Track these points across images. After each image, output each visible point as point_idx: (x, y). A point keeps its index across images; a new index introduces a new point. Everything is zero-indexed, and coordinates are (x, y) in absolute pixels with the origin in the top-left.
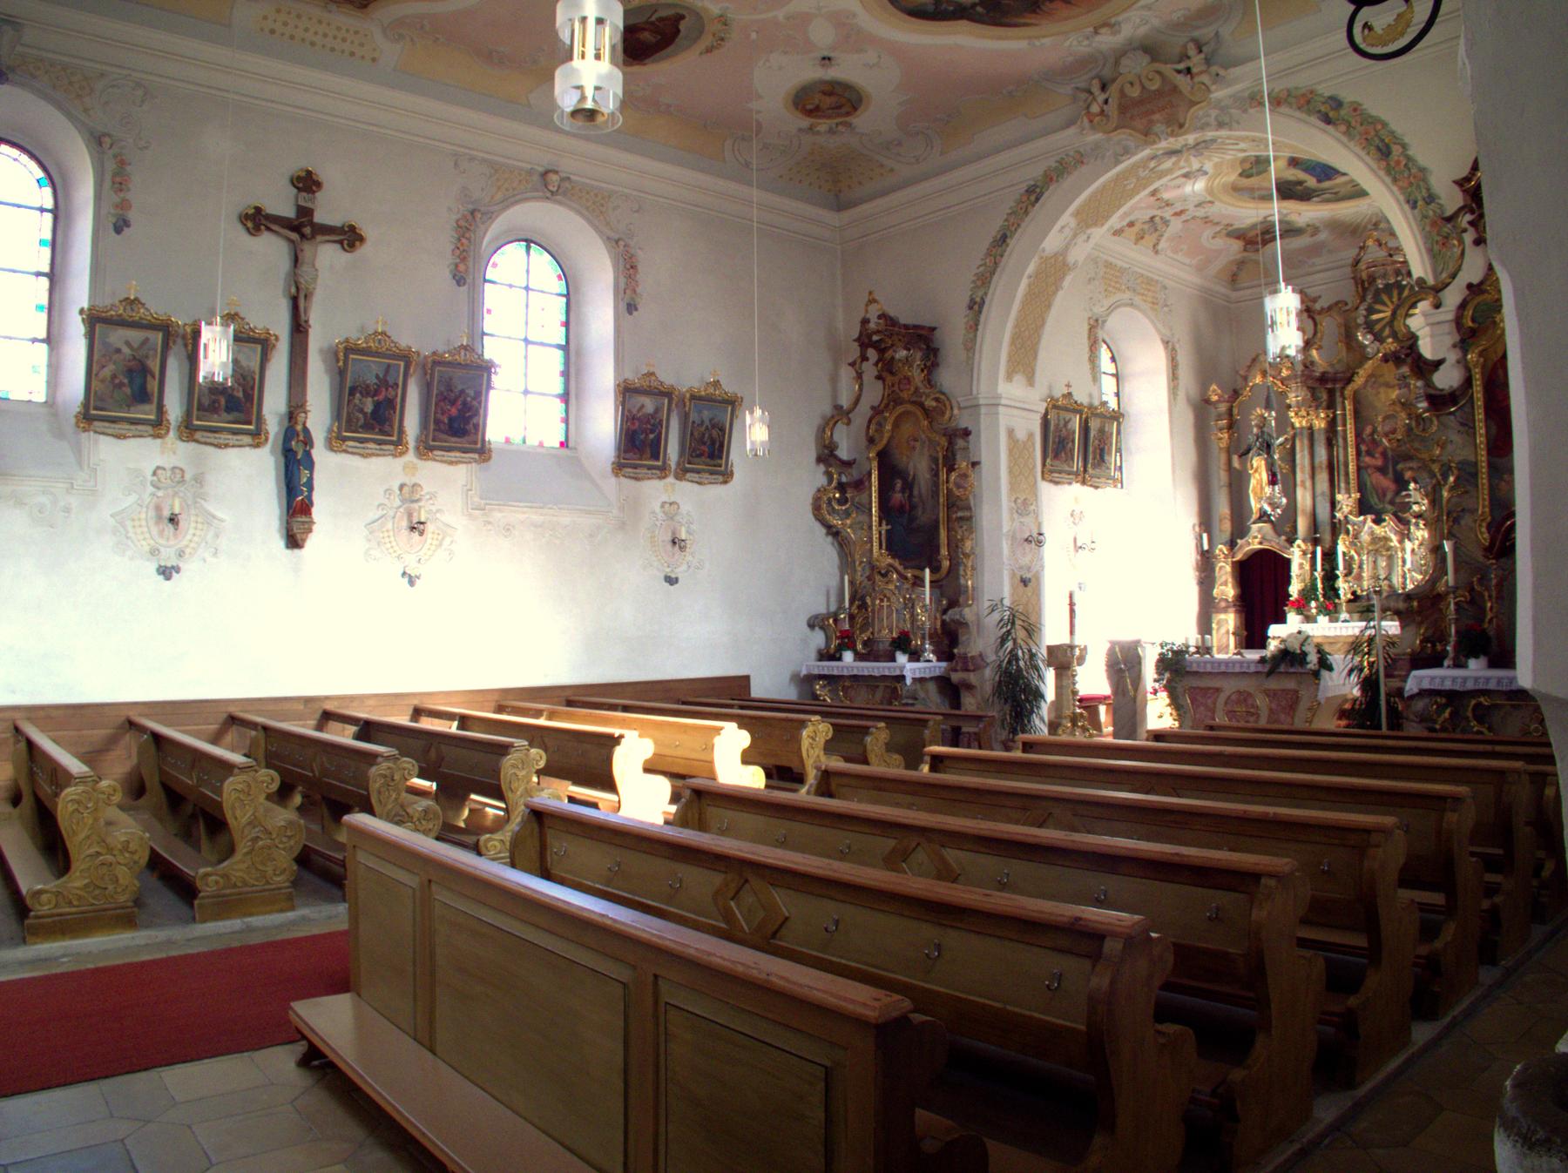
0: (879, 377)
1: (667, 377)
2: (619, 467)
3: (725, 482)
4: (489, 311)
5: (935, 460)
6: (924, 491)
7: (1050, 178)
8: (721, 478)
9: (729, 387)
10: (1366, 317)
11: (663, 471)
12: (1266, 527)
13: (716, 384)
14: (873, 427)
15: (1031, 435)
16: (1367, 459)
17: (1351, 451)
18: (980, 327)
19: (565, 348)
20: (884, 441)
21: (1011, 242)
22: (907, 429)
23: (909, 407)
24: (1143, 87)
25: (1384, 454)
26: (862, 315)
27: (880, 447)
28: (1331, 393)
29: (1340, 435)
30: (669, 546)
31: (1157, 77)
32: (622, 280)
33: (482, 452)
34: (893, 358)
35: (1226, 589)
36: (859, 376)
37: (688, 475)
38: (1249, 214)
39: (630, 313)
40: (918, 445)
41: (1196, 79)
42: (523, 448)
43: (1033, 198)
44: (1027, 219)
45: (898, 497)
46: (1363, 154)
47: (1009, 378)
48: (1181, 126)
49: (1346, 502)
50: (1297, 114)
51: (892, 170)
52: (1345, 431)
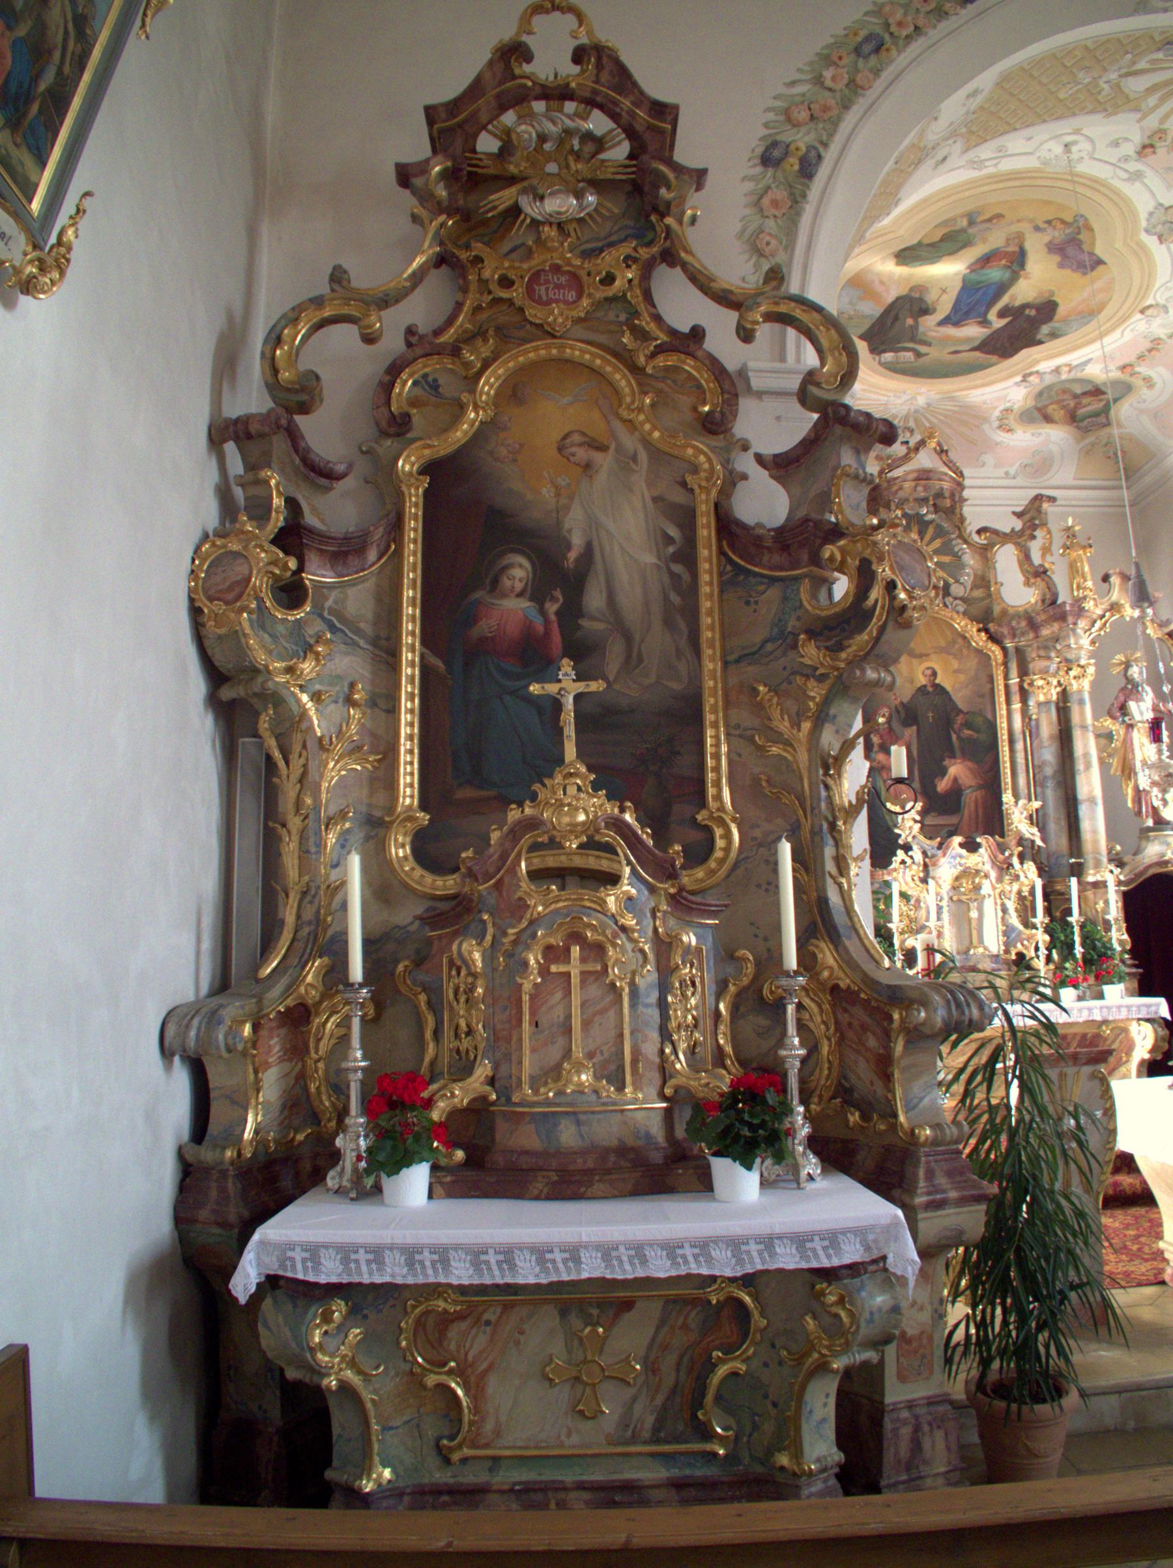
6: (631, 599)
14: (405, 386)
20: (462, 433)
22: (557, 414)
40: (605, 462)
45: (511, 605)
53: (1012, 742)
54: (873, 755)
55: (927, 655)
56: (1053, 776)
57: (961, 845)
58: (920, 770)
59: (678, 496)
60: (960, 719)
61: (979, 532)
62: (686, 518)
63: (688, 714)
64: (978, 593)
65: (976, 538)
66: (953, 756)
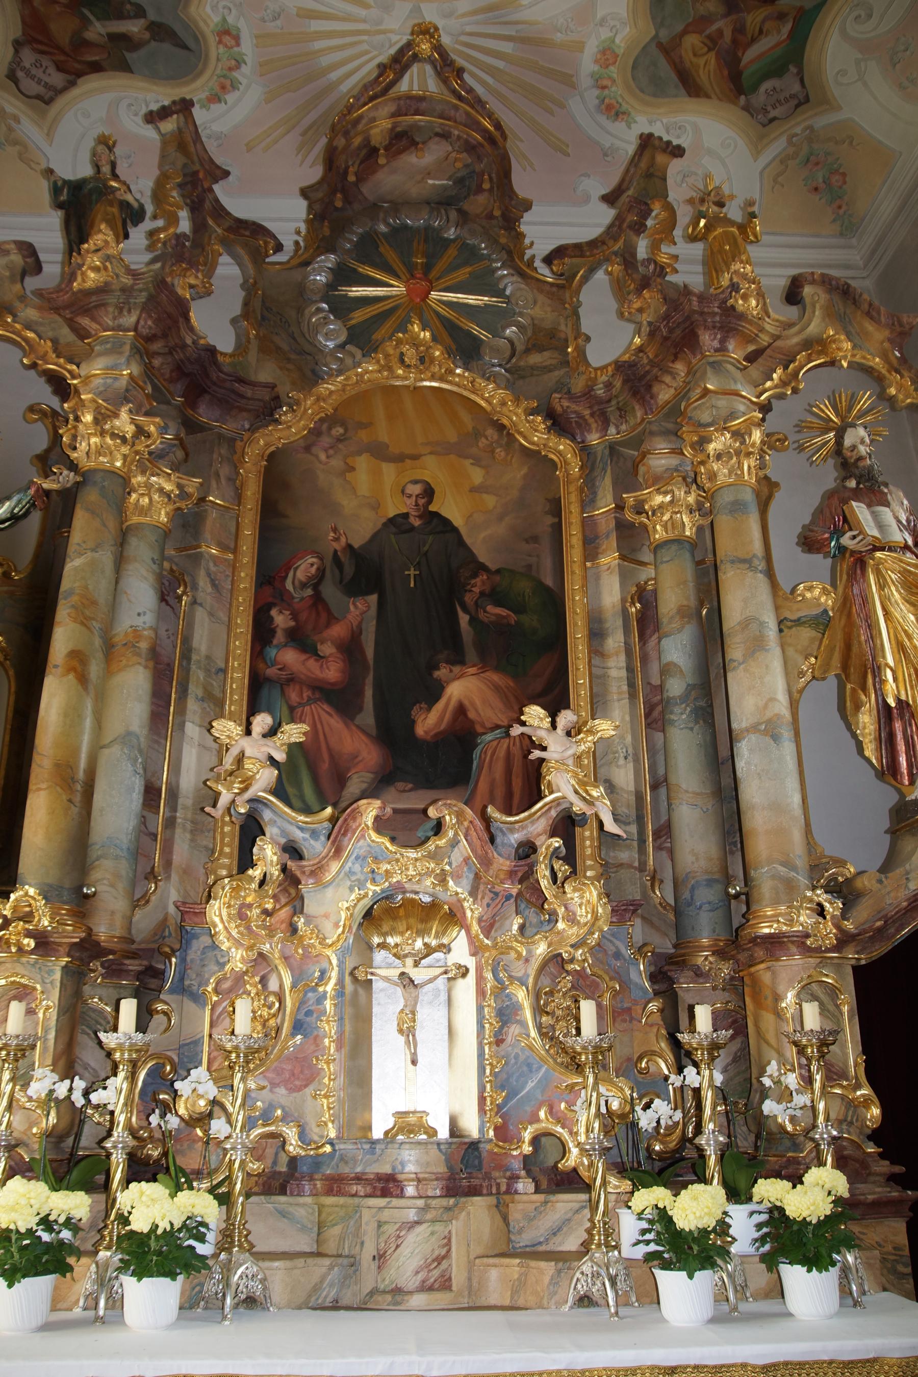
10: (331, 286)
16: (290, 657)
25: (350, 648)
53: (596, 634)
54: (272, 652)
55: (415, 457)
56: (684, 698)
57: (380, 825)
58: (378, 687)
60: (479, 584)
61: (548, 260)
66: (458, 658)
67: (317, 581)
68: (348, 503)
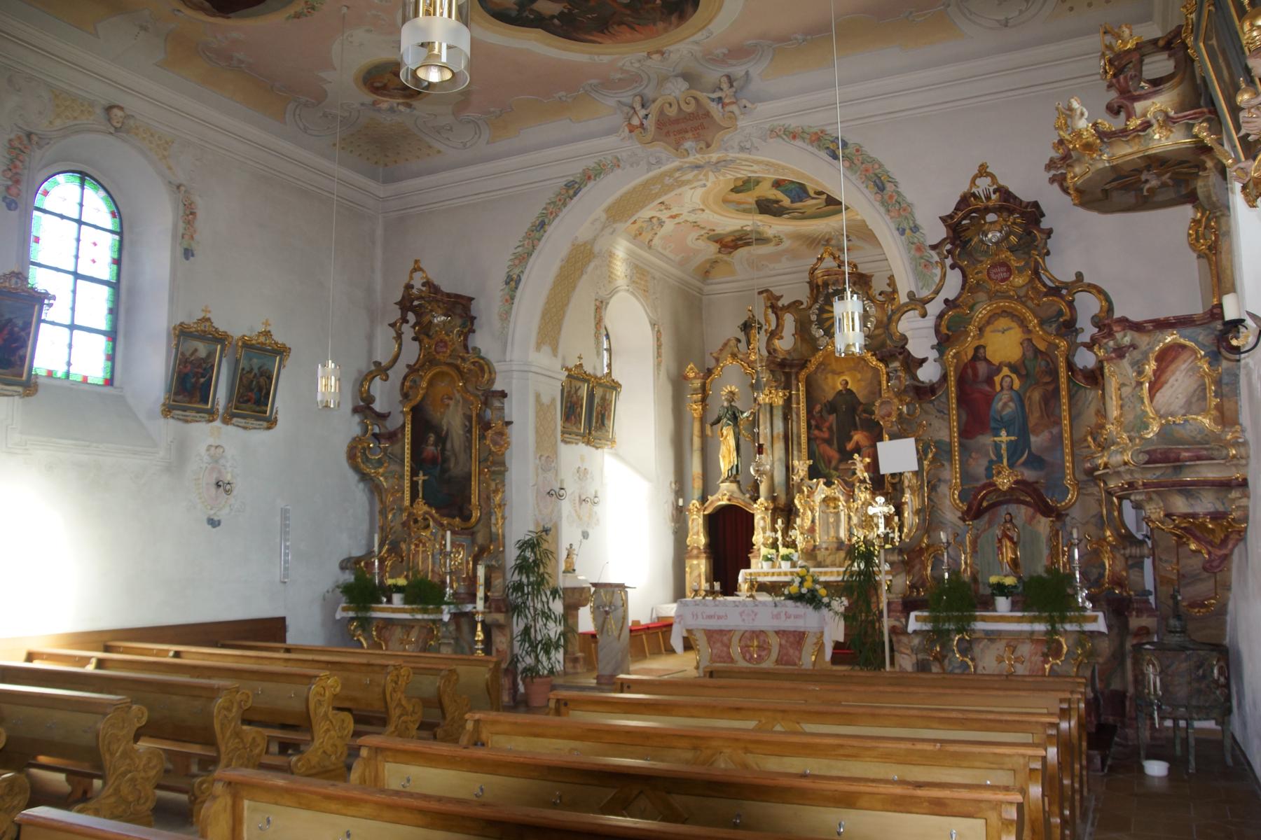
0: (415, 339)
1: (221, 324)
2: (168, 410)
3: (269, 428)
4: (37, 240)
5: (469, 418)
7: (588, 176)
8: (265, 424)
9: (279, 337)
11: (211, 415)
12: (734, 486)
13: (267, 334)
14: (407, 384)
15: (554, 400)
16: (816, 432)
17: (803, 425)
18: (516, 301)
19: (115, 286)
20: (419, 398)
21: (550, 229)
22: (442, 387)
23: (445, 369)
24: (680, 109)
25: (830, 429)
26: (405, 280)
27: (414, 403)
28: (788, 376)
29: (794, 410)
30: (213, 490)
31: (693, 101)
32: (181, 225)
33: (29, 386)
34: (431, 322)
35: (698, 537)
36: (399, 337)
37: (235, 420)
38: (731, 223)
39: (187, 258)
40: (452, 403)
41: (728, 108)
42: (66, 383)
43: (571, 192)
44: (565, 210)
45: (430, 449)
46: (862, 187)
47: (538, 347)
48: (708, 146)
49: (801, 466)
50: (810, 148)
51: (439, 152)
52: (798, 409)
59: (468, 413)
60: (861, 408)
62: (469, 418)
63: (468, 478)
64: (877, 332)
65: (881, 298)
66: (856, 429)
67: (821, 411)
68: (826, 388)
